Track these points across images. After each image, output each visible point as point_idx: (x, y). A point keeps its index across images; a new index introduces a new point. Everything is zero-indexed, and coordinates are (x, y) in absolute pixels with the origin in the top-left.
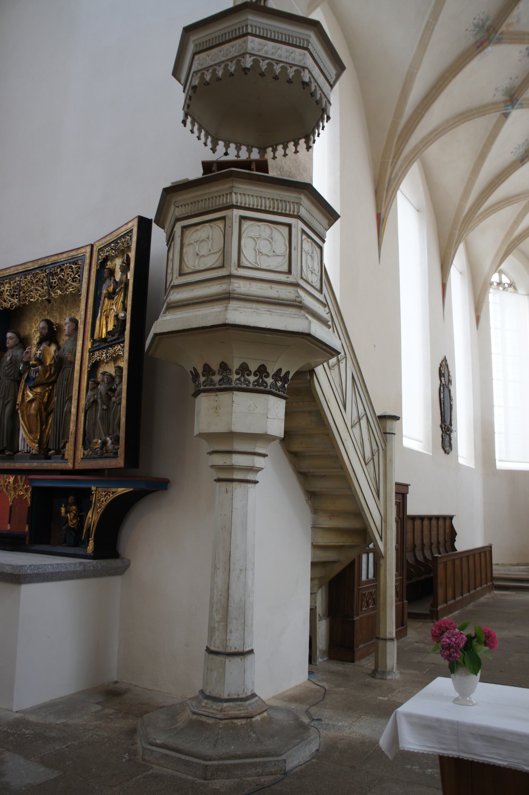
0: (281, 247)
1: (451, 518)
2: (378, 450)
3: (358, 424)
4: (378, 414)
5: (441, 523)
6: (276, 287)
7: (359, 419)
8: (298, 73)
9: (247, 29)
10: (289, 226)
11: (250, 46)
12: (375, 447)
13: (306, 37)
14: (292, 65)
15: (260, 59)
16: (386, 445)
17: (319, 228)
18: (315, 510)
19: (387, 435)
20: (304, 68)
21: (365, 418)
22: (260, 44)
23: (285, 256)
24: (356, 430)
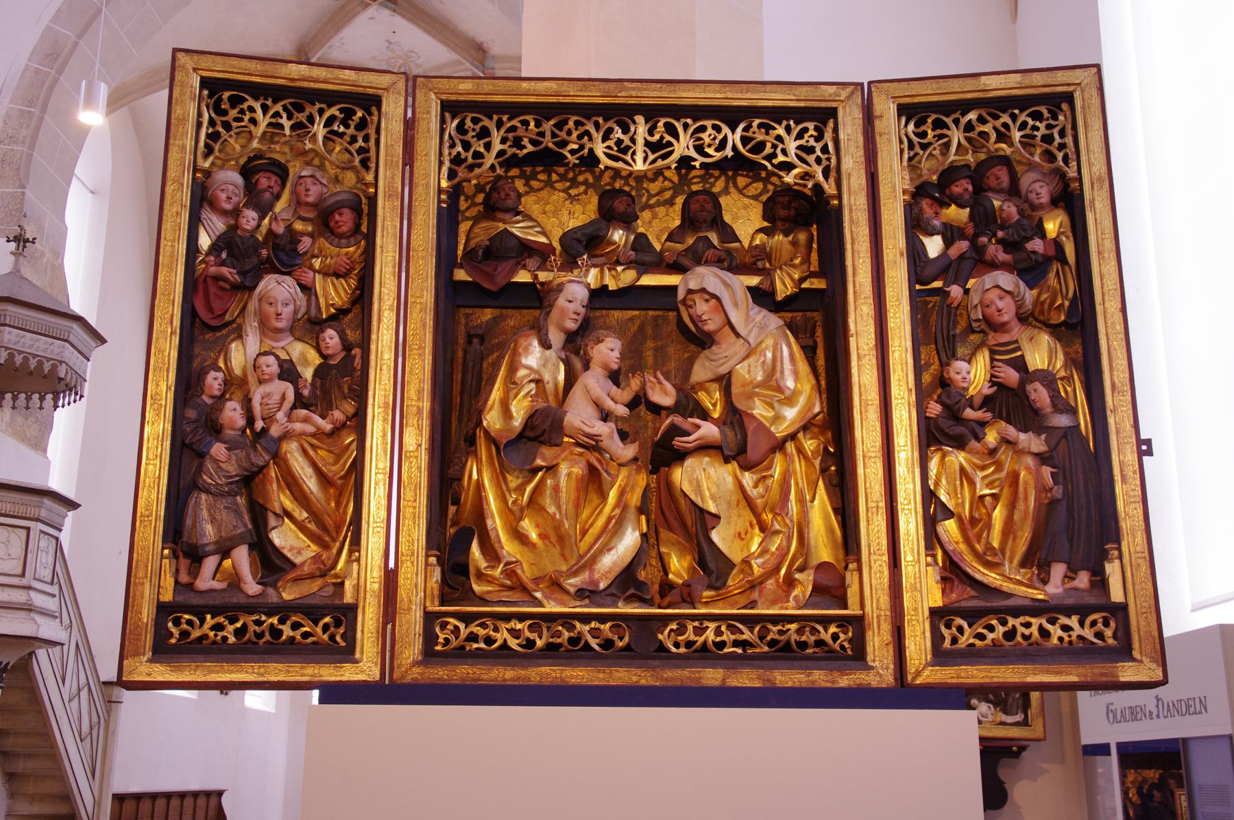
0: (17, 549)
1: (220, 794)
2: (99, 722)
3: (77, 698)
4: (103, 679)
5: (201, 802)
6: (7, 590)
7: (79, 690)
8: (54, 367)
9: (5, 319)
10: (28, 529)
11: (6, 337)
12: (95, 719)
13: (68, 329)
14: (49, 359)
15: (15, 352)
16: (109, 716)
17: (55, 519)
18: (12, 795)
19: (113, 704)
20: (61, 362)
21: (86, 689)
22: (18, 335)
23: (19, 559)
24: (74, 704)
